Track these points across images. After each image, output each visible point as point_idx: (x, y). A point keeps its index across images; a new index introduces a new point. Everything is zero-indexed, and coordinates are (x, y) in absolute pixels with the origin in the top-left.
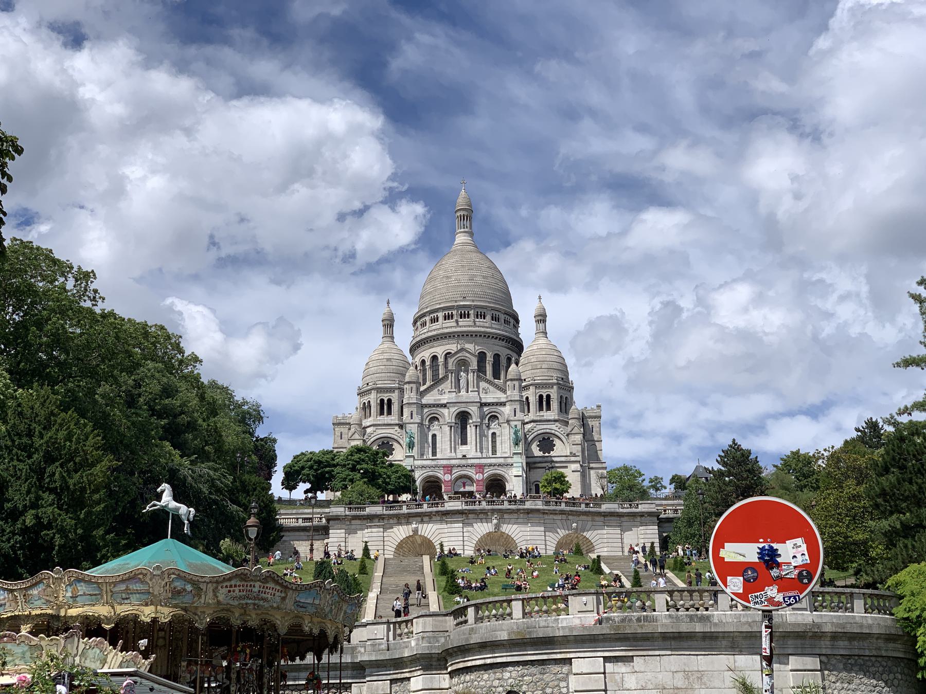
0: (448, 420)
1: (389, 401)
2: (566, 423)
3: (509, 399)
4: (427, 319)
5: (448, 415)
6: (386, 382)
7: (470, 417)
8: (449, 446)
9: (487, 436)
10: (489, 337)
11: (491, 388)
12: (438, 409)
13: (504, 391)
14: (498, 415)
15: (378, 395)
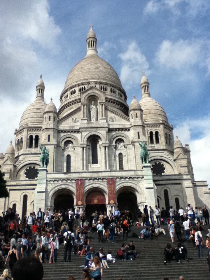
0: (80, 142)
1: (37, 137)
2: (172, 153)
3: (133, 124)
4: (69, 93)
5: (81, 138)
6: (35, 123)
7: (99, 141)
8: (82, 164)
9: (115, 156)
10: (109, 101)
11: (117, 117)
12: (72, 134)
13: (128, 120)
14: (124, 139)
15: (29, 133)
